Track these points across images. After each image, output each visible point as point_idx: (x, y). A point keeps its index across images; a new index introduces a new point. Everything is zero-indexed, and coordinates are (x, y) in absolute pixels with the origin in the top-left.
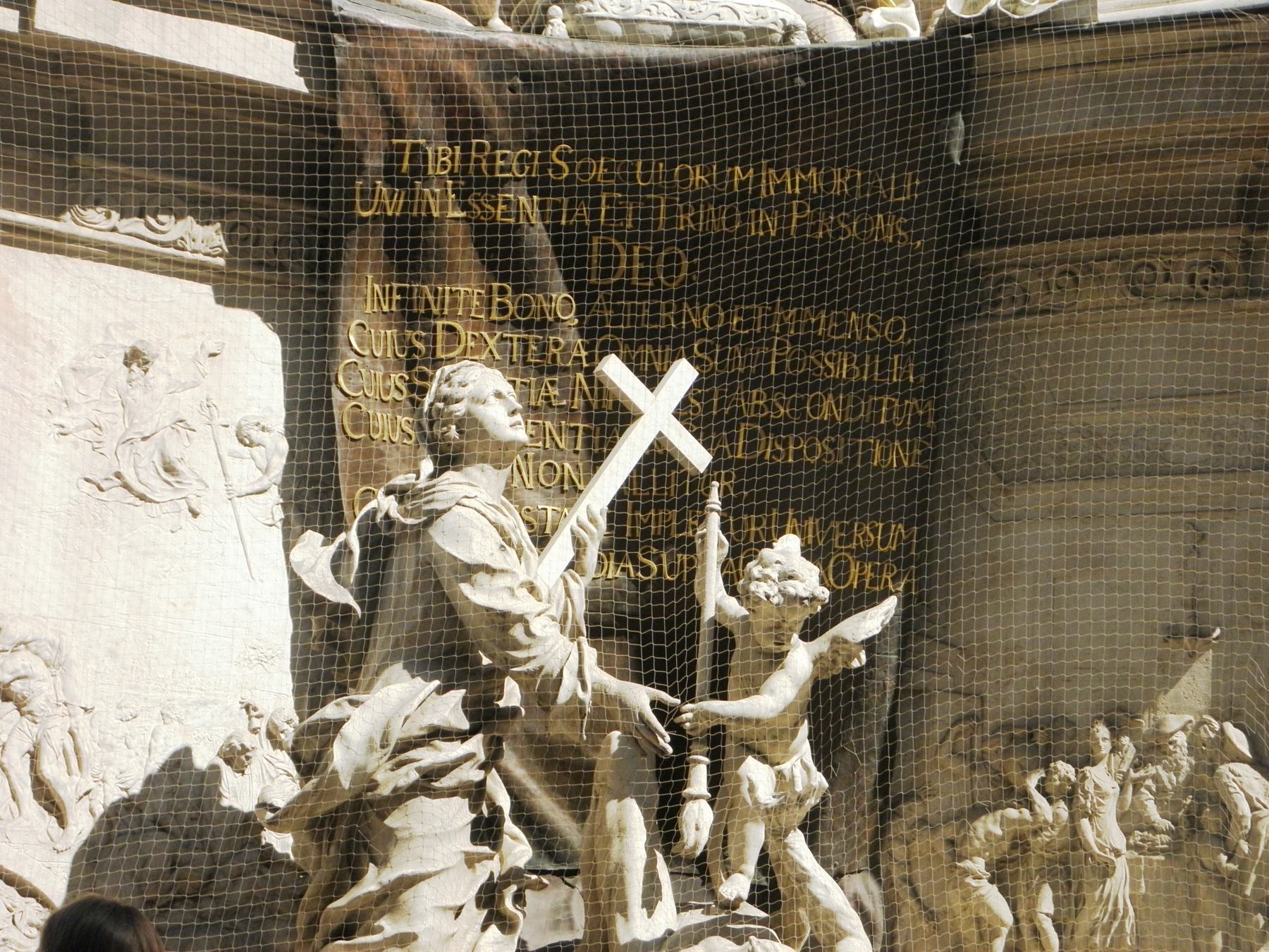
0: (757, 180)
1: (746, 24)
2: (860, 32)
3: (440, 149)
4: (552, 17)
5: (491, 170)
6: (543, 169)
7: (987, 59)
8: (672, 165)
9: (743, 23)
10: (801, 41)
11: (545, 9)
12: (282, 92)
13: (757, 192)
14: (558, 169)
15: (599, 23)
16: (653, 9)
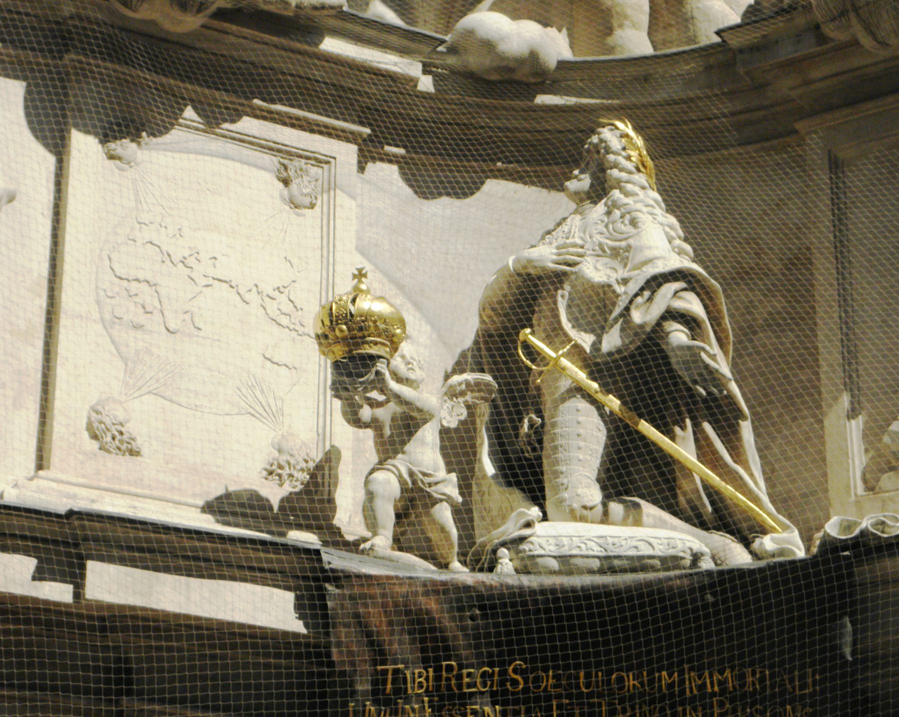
0: (682, 682)
1: (660, 554)
3: (417, 671)
4: (500, 558)
5: (460, 686)
6: (502, 683)
7: (865, 571)
8: (609, 673)
9: (658, 553)
10: (707, 564)
11: (494, 551)
12: (286, 634)
13: (682, 692)
14: (515, 683)
15: (539, 560)
16: (583, 546)
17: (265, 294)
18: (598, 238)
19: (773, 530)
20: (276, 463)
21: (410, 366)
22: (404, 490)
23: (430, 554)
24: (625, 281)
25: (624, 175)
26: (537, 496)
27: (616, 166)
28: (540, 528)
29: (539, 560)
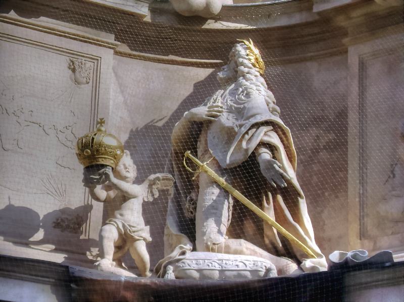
1: (249, 269)
2: (300, 268)
9: (248, 268)
10: (274, 274)
11: (165, 267)
15: (188, 271)
16: (210, 265)
17: (59, 130)
18: (229, 102)
19: (313, 257)
20: (60, 219)
21: (127, 170)
22: (120, 234)
23: (132, 268)
24: (241, 126)
25: (246, 70)
26: (192, 238)
27: (242, 64)
28: (189, 255)
29: (188, 271)
